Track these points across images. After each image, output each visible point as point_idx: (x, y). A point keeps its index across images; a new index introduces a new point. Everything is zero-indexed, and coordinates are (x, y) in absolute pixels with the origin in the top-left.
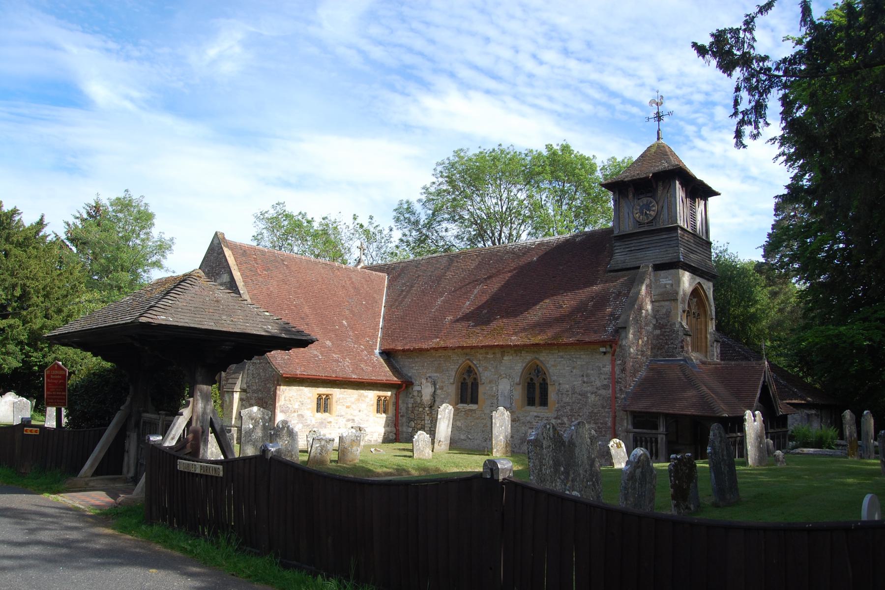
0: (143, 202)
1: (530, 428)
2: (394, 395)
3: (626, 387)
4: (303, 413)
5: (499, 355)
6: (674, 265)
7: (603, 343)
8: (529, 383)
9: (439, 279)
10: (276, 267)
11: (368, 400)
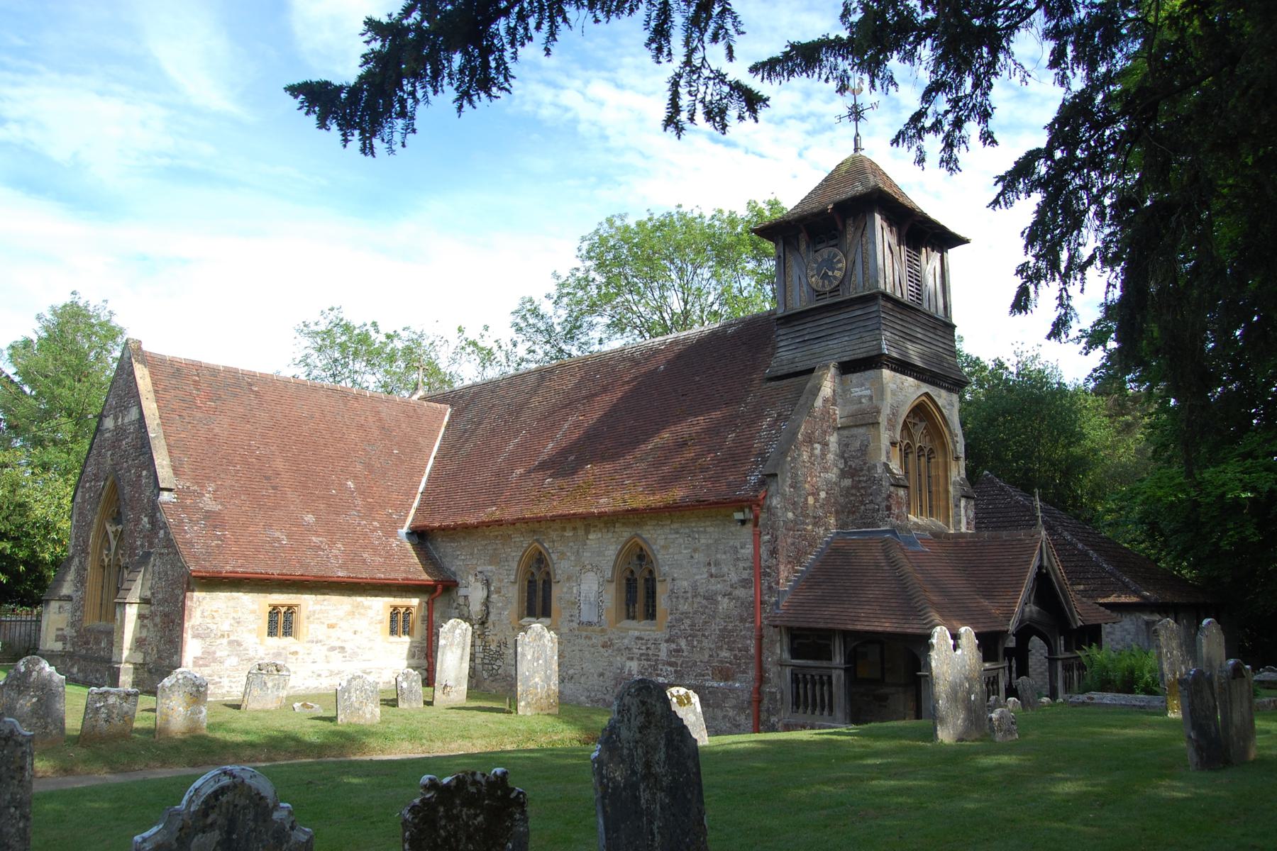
0: (108, 310)
1: (628, 659)
2: (424, 604)
3: (778, 583)
4: (235, 638)
5: (581, 532)
6: (873, 362)
7: (739, 504)
8: (628, 580)
9: (520, 408)
10: (236, 395)
11: (371, 613)
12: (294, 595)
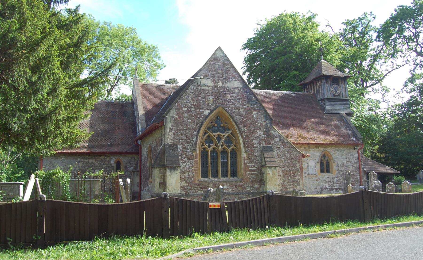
5: (307, 148)
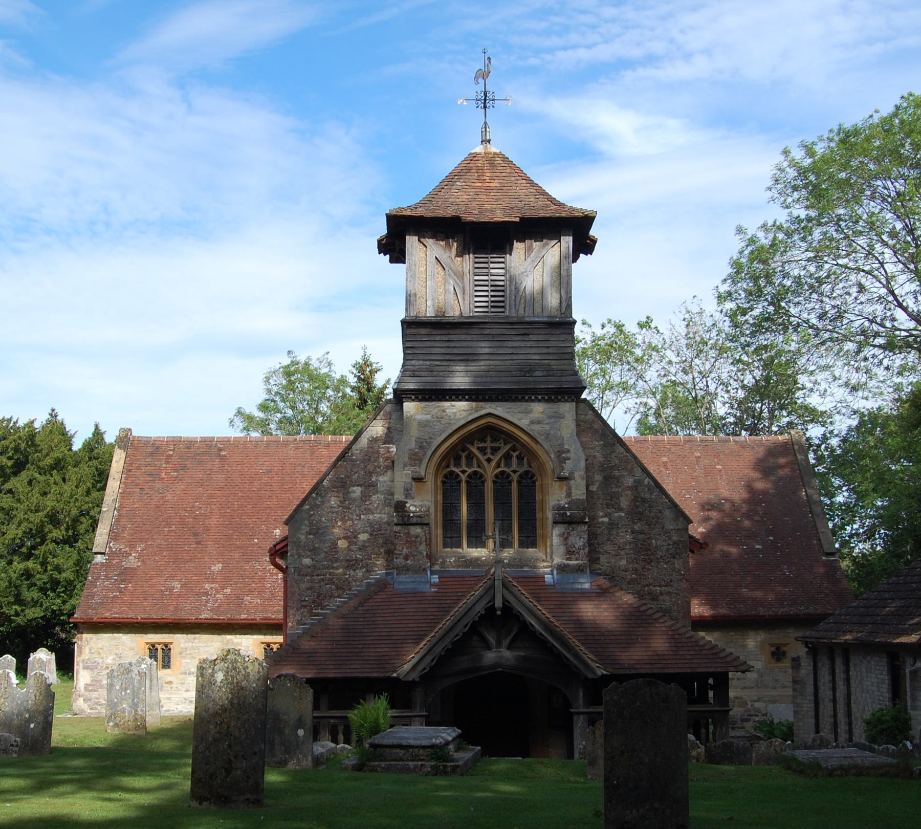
12: (168, 635)
